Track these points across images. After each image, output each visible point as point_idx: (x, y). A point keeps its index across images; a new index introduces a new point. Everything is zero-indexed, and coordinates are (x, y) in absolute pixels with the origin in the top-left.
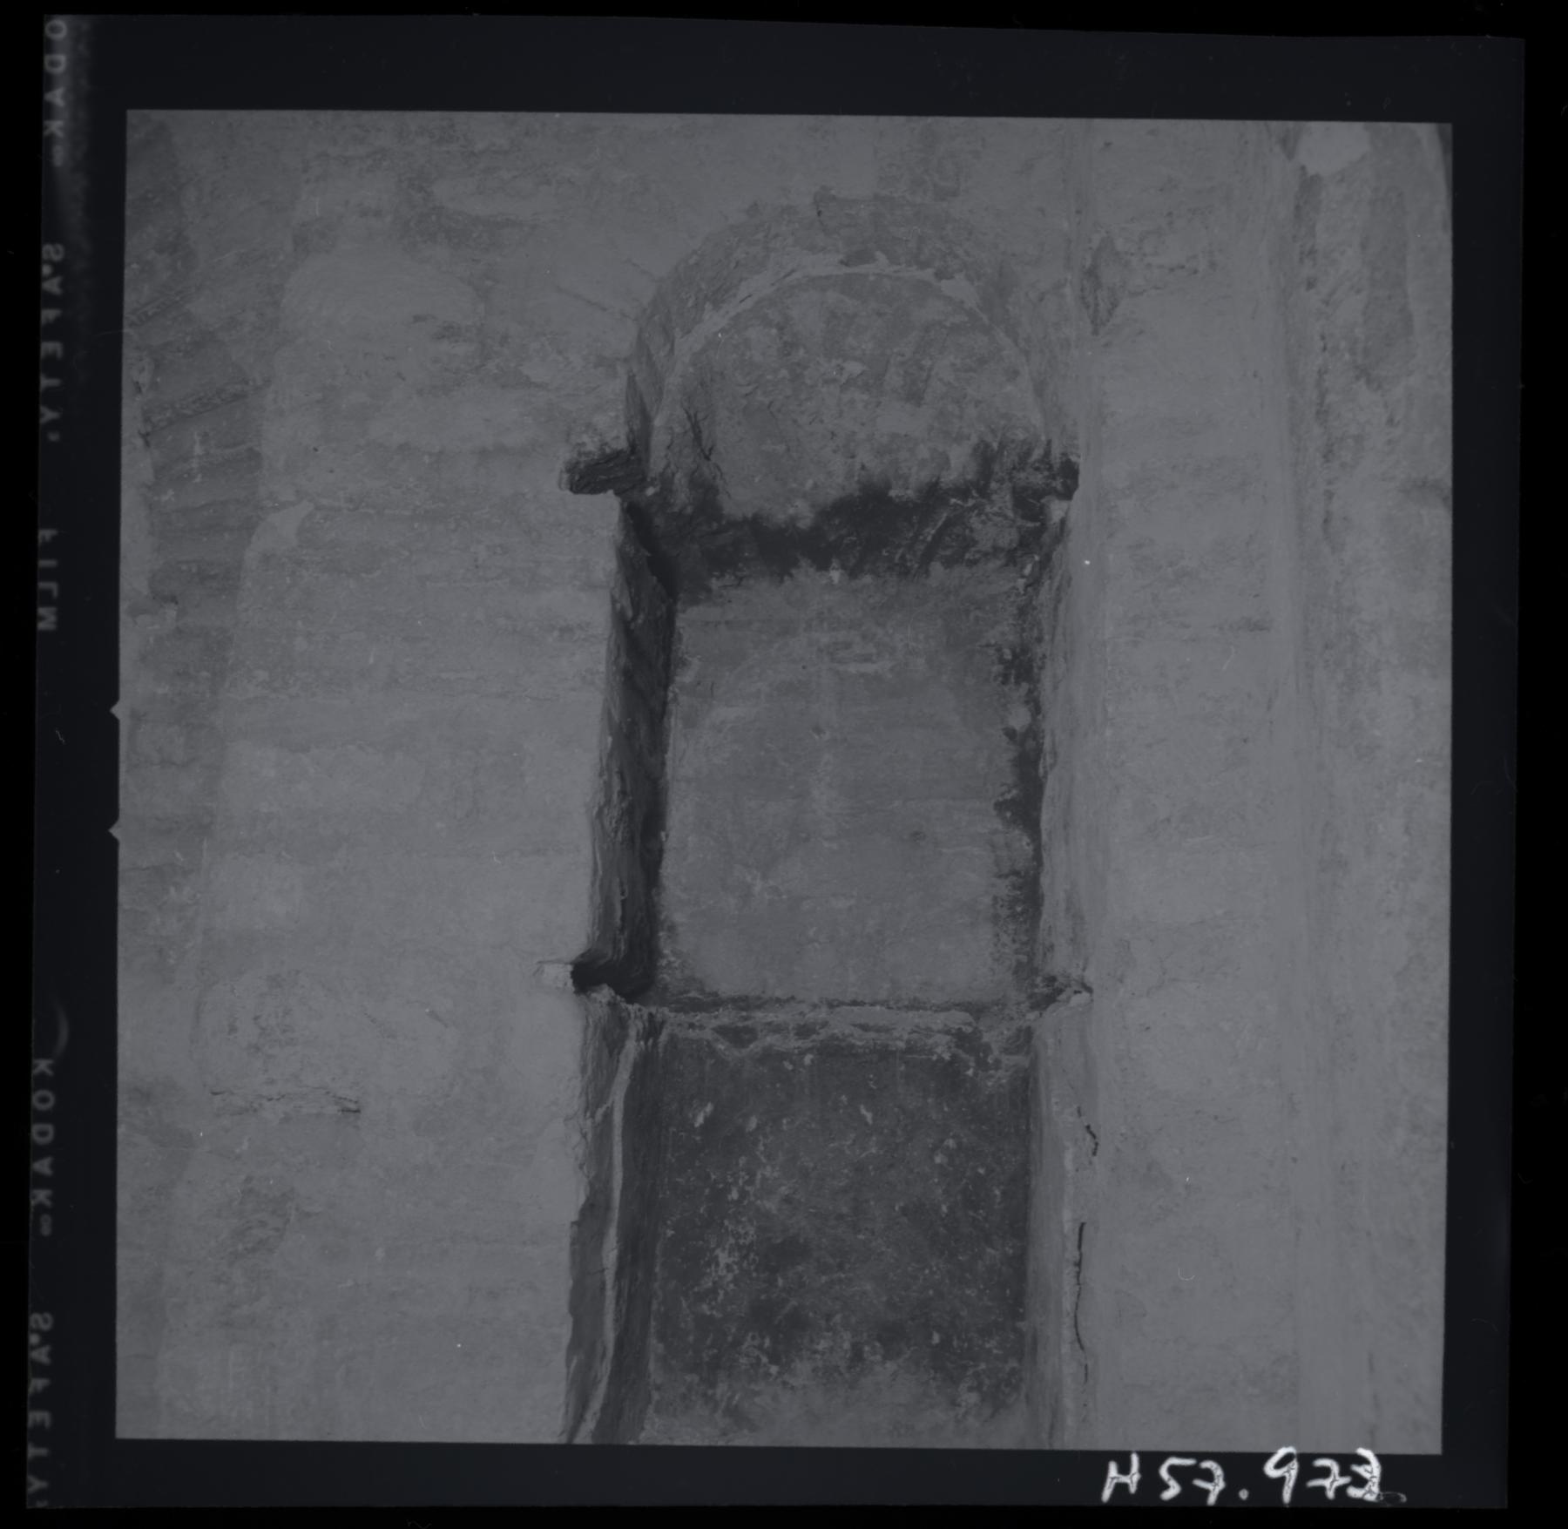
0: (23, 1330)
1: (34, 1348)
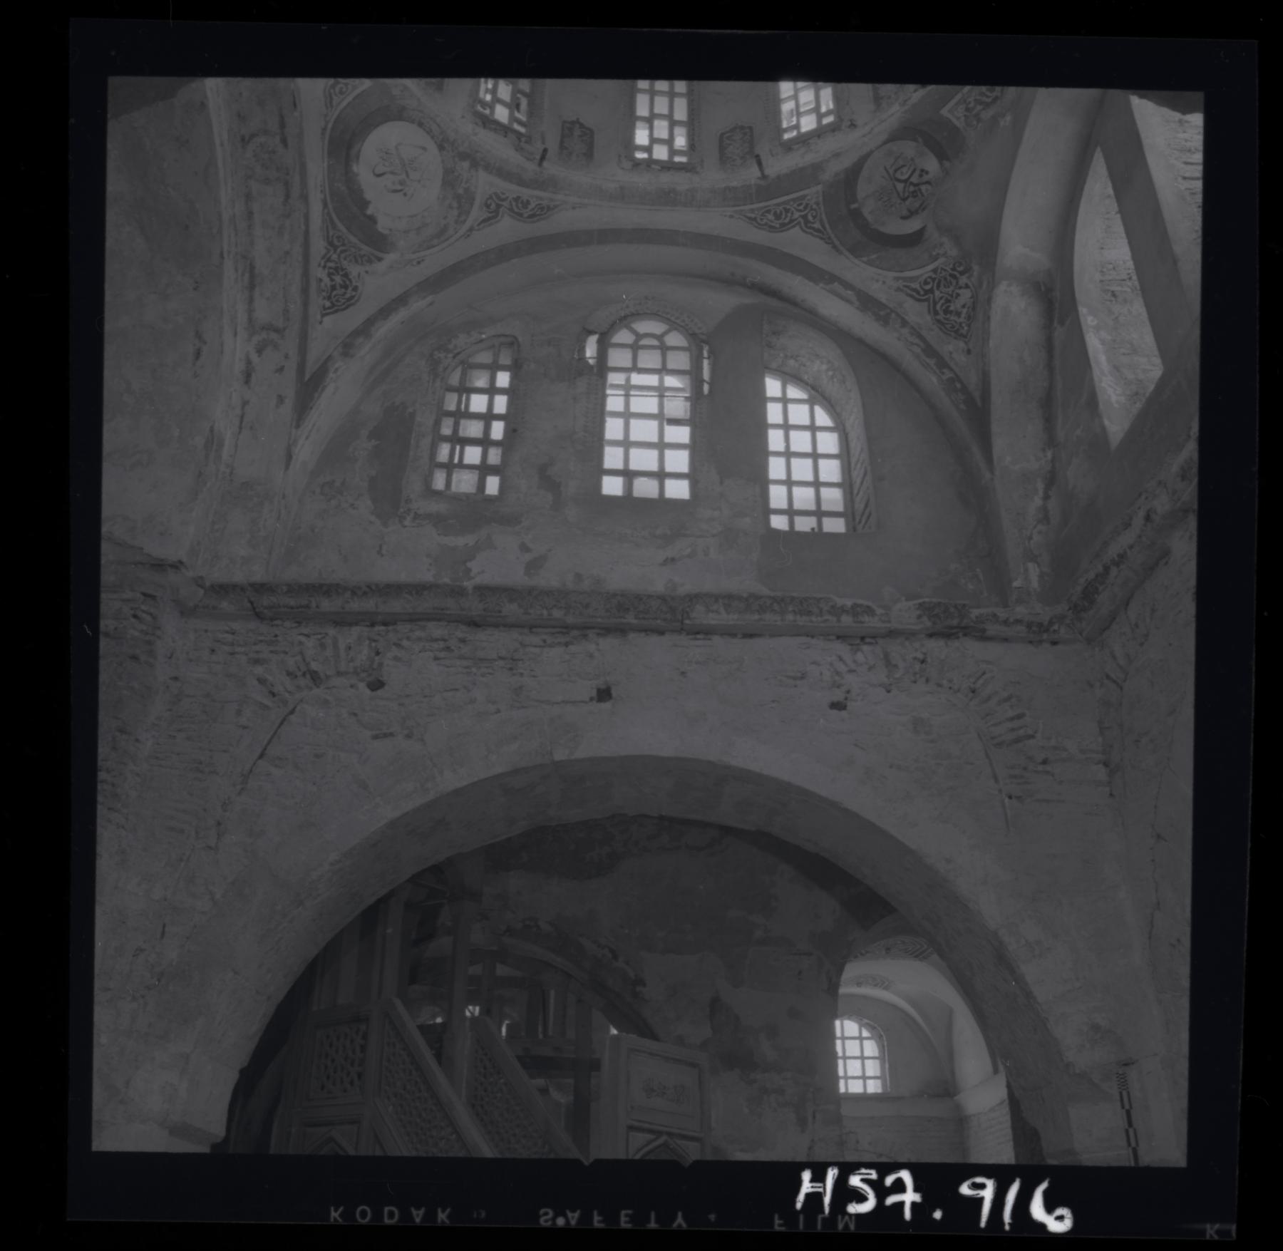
0: (554, 1231)
1: (568, 1222)
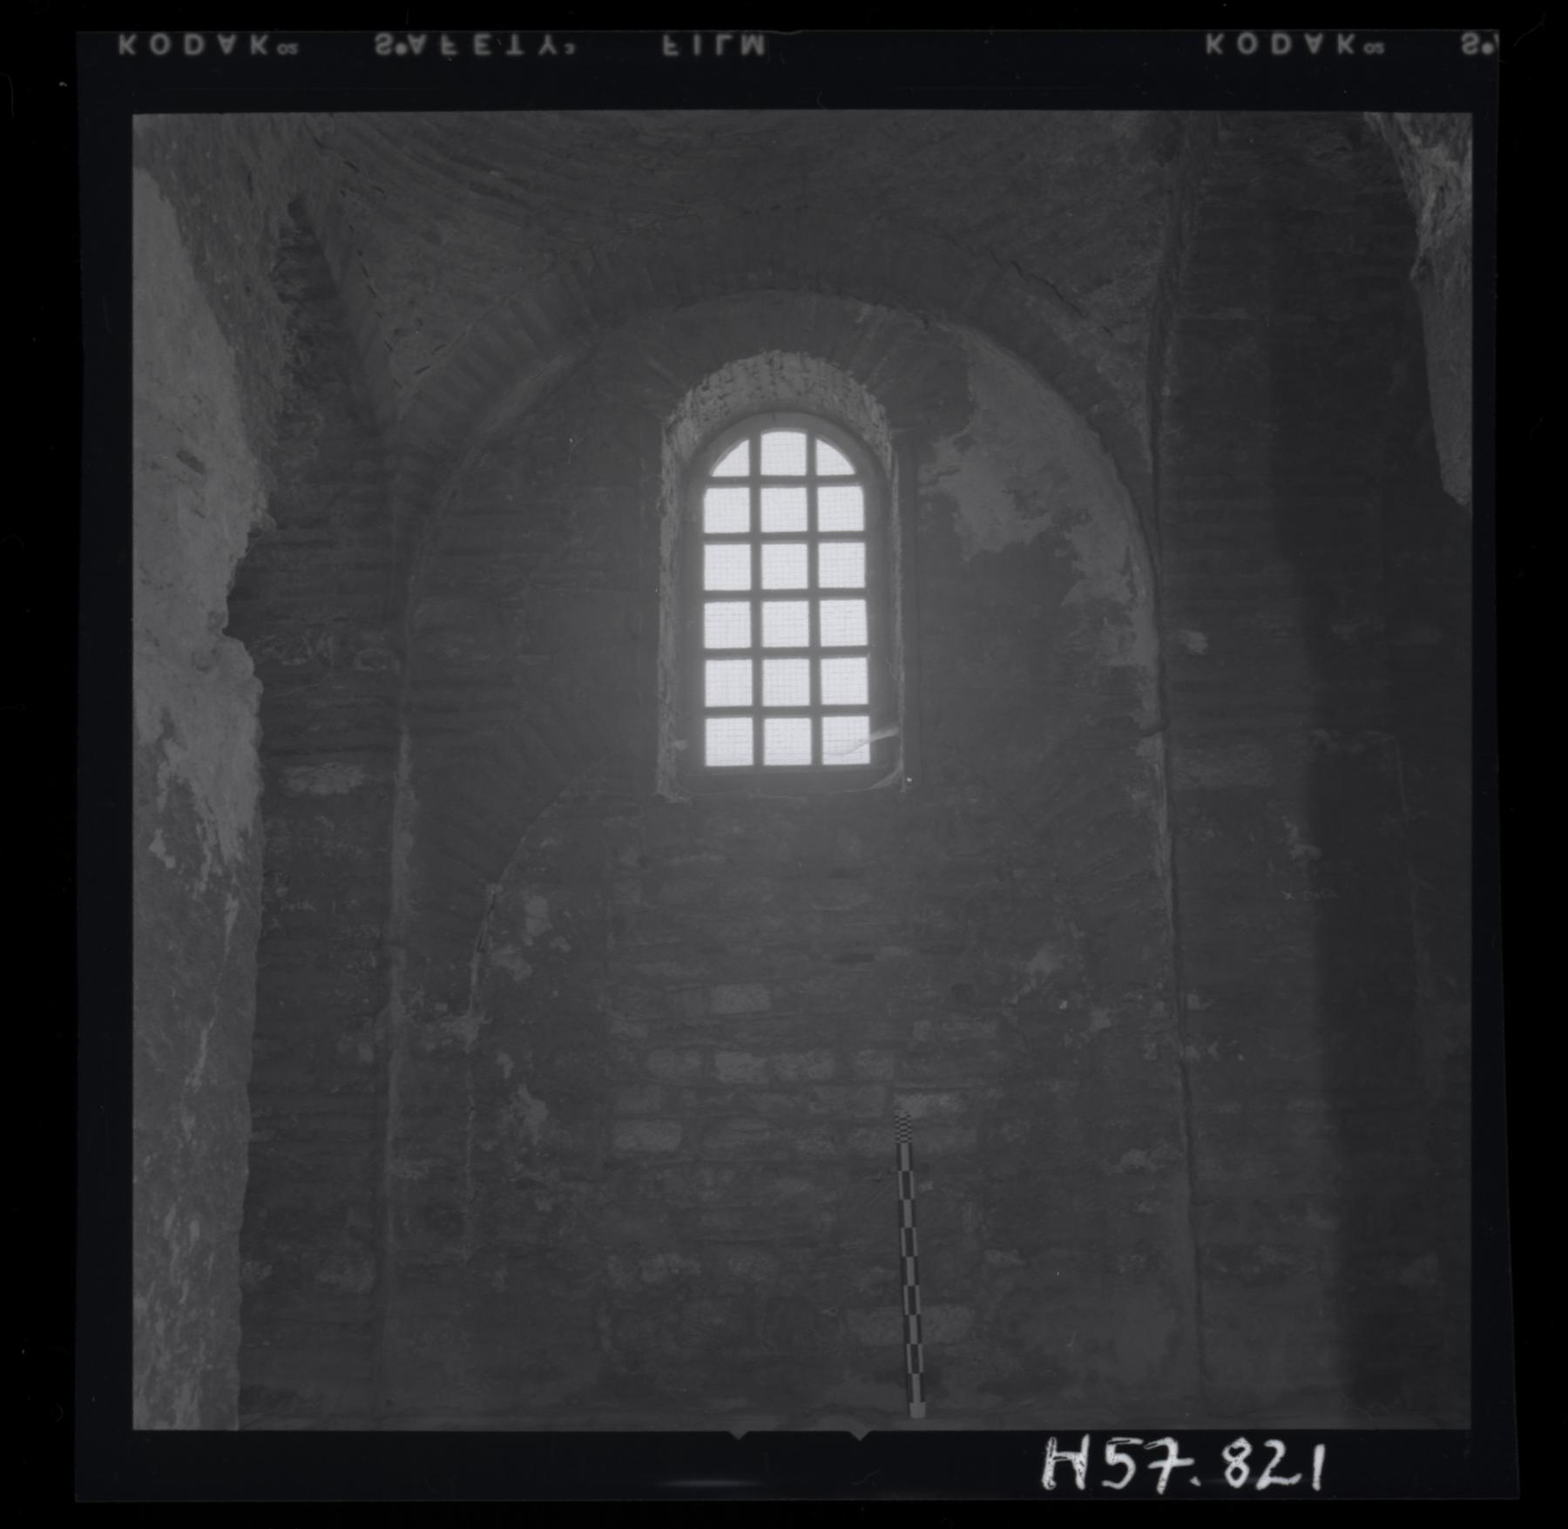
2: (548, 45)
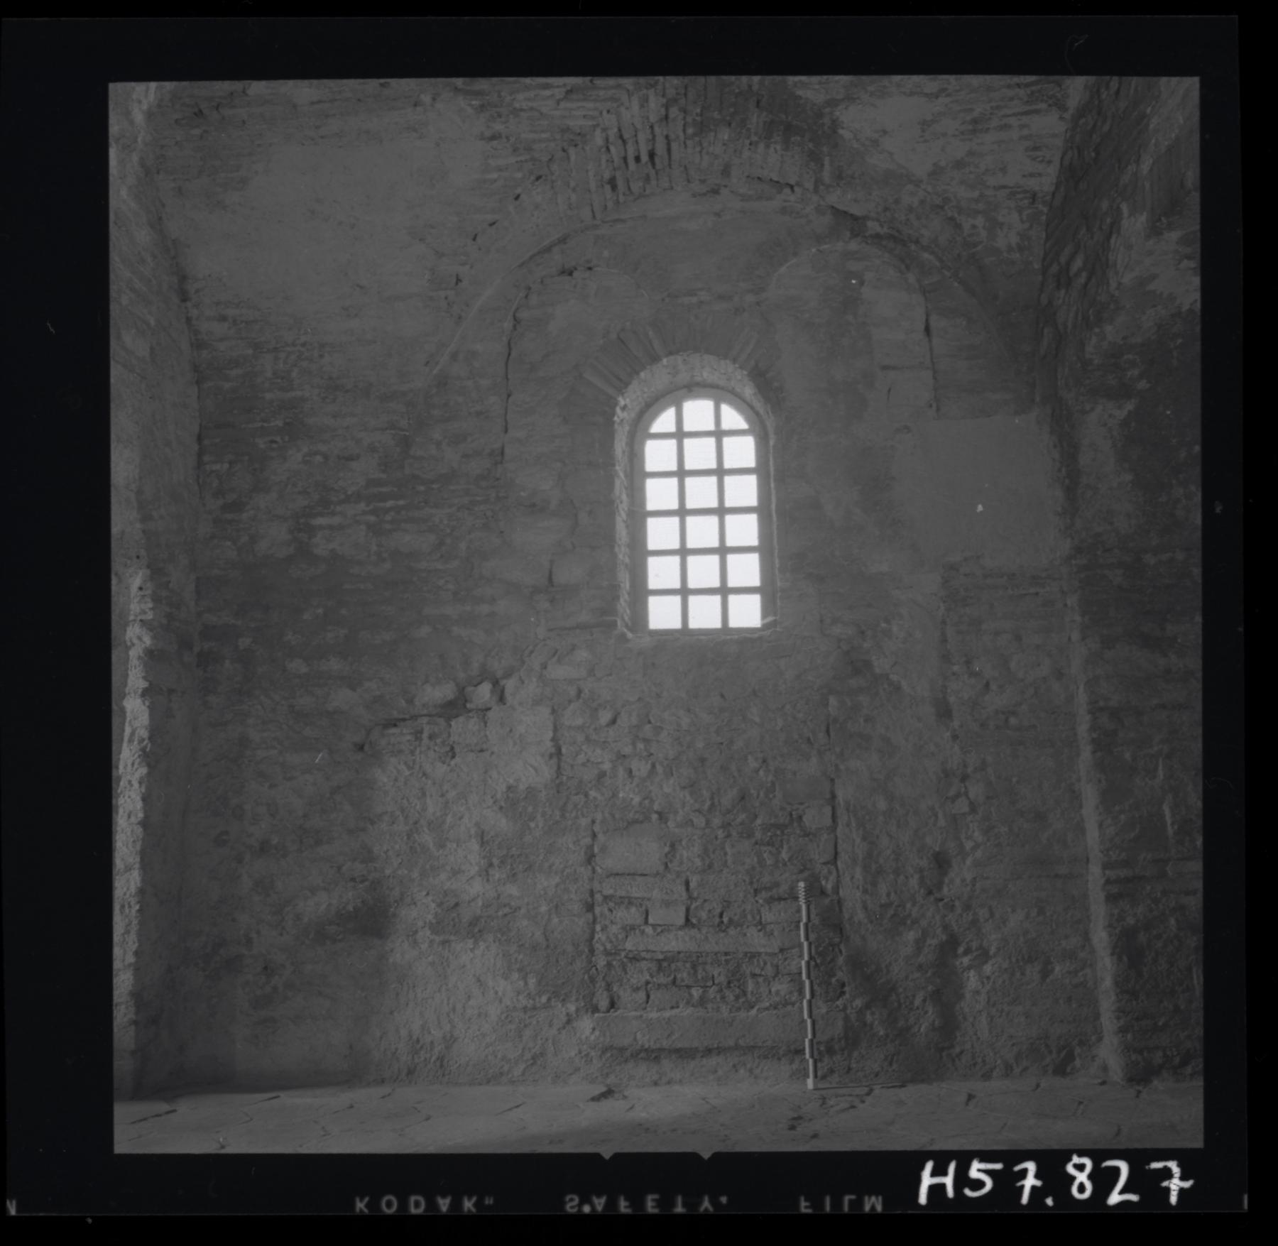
0: (580, 1217)
2: (706, 1205)
